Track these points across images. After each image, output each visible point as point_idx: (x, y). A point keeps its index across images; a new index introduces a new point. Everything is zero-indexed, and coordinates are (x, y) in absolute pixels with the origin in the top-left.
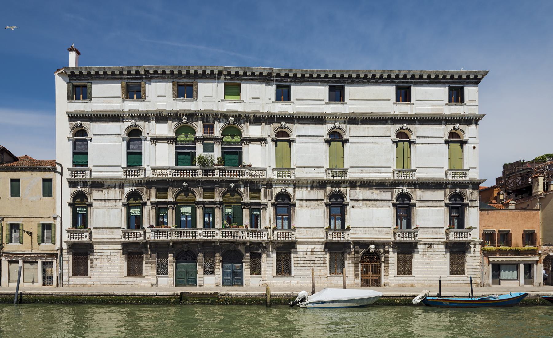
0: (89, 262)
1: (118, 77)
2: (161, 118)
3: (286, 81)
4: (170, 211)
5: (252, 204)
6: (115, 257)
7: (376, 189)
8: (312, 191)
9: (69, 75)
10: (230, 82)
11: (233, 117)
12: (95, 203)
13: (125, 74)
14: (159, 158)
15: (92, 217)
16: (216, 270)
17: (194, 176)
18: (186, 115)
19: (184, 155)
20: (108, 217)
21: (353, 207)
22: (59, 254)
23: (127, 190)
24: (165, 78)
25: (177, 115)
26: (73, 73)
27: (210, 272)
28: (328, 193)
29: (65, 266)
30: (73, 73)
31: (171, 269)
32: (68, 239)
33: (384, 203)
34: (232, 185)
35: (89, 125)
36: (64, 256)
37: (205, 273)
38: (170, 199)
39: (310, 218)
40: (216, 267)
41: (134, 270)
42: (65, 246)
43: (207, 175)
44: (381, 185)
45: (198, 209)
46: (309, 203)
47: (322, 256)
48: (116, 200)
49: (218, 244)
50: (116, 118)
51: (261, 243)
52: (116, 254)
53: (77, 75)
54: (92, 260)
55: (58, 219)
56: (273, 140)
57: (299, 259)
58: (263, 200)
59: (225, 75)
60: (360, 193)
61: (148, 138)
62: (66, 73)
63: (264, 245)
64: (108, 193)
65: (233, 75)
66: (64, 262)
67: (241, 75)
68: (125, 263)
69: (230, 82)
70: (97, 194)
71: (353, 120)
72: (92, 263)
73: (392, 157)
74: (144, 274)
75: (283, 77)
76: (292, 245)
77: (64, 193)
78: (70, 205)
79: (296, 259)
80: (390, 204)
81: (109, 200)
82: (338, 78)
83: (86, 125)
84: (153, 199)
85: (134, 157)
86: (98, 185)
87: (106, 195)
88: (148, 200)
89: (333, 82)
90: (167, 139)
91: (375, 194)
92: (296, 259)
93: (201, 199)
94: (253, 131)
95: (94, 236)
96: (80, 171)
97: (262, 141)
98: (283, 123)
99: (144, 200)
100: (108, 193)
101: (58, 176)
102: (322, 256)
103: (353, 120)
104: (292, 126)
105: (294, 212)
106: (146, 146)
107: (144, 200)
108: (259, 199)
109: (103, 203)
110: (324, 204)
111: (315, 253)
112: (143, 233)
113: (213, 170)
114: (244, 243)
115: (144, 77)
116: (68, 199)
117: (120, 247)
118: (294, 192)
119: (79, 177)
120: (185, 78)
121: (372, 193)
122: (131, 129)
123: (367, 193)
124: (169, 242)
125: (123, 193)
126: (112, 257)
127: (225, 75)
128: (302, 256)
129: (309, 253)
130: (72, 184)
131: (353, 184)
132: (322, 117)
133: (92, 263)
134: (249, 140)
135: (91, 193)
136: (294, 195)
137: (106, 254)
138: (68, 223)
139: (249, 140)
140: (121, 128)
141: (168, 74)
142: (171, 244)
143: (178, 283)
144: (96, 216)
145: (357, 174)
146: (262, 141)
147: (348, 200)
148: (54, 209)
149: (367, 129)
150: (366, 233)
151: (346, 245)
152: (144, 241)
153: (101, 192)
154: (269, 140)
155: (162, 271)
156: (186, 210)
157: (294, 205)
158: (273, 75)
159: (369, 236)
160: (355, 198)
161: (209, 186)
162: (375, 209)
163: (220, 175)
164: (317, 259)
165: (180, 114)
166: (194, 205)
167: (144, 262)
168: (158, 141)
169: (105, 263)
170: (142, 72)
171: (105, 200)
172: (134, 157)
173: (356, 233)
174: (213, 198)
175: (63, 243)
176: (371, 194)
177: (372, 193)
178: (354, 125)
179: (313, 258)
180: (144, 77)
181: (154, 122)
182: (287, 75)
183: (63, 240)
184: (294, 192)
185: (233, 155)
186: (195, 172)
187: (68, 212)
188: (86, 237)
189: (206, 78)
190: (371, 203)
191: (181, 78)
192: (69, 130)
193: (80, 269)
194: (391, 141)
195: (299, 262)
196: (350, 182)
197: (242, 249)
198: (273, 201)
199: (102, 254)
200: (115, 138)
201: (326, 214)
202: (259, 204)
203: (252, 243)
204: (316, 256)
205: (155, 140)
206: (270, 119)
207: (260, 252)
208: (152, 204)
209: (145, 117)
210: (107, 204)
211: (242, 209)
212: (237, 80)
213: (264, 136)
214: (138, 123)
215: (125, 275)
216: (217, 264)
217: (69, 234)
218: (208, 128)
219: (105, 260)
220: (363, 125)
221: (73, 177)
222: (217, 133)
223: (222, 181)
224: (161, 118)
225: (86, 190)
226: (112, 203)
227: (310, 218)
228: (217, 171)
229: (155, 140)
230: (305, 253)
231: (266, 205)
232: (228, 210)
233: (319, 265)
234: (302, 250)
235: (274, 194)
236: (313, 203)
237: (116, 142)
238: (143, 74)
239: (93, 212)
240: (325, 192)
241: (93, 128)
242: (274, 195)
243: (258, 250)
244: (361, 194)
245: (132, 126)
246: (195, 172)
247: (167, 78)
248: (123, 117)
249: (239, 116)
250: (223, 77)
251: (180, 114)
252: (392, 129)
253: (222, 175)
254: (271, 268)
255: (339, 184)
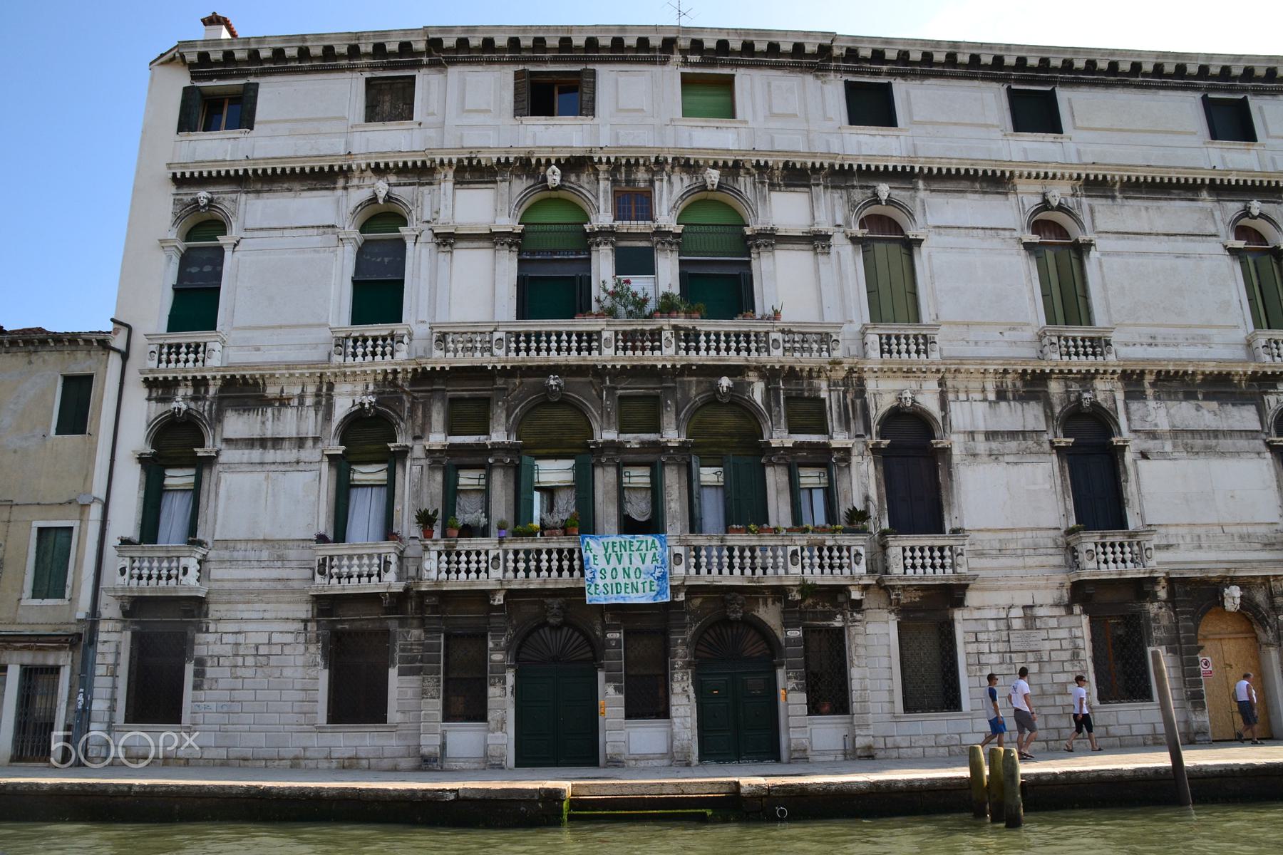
0: (189, 669)
1: (344, 62)
2: (472, 172)
3: (877, 74)
4: (498, 478)
5: (798, 447)
6: (287, 650)
7: (1207, 397)
8: (1003, 404)
9: (191, 65)
10: (698, 71)
11: (715, 166)
12: (228, 455)
13: (367, 55)
14: (464, 295)
15: (212, 504)
16: (674, 700)
17: (584, 353)
18: (558, 163)
19: (550, 286)
20: (268, 500)
21: (1144, 455)
22: (85, 638)
23: (342, 407)
24: (490, 62)
25: (529, 160)
26: (204, 56)
27: (647, 702)
28: (1058, 410)
29: (101, 684)
30: (204, 56)
31: (502, 699)
32: (122, 581)
33: (1242, 443)
34: (725, 382)
35: (234, 201)
36: (100, 648)
37: (633, 712)
38: (498, 436)
39: (1006, 498)
40: (677, 687)
41: (356, 699)
42: (110, 609)
43: (634, 349)
44: (1219, 386)
45: (598, 472)
46: (994, 445)
47: (1063, 633)
48: (300, 442)
49: (681, 597)
50: (323, 177)
51: (844, 589)
52: (289, 638)
53: (217, 63)
54: (200, 663)
55: (95, 512)
56: (854, 240)
57: (985, 648)
58: (839, 439)
59: (684, 52)
60: (1160, 414)
61: (427, 236)
62: (182, 56)
63: (856, 595)
64: (276, 418)
65: (710, 50)
66: (100, 670)
67: (734, 52)
68: (324, 676)
69: (698, 71)
70: (236, 424)
71: (1097, 186)
72: (200, 674)
73: (1235, 299)
74: (393, 715)
75: (865, 60)
76: (954, 594)
77: (128, 420)
78: (142, 459)
79: (973, 648)
80: (1259, 444)
81: (277, 442)
82: (1032, 69)
83: (227, 198)
84: (437, 439)
85: (378, 295)
86: (244, 392)
87: (269, 424)
88: (416, 438)
89: (1019, 81)
90: (494, 238)
91: (1205, 415)
92: (973, 648)
93: (611, 435)
94: (786, 210)
95: (216, 573)
96: (188, 346)
97: (816, 241)
98: (884, 189)
99: (402, 441)
100: (276, 418)
101: (114, 361)
102: (1063, 633)
103: (1097, 186)
104: (913, 198)
105: (950, 475)
106: (419, 261)
107: (402, 441)
108: (823, 430)
109: (256, 454)
110: (1047, 446)
111: (1038, 623)
112: (393, 558)
113: (652, 333)
114: (779, 592)
115: (425, 59)
116: (135, 438)
117: (304, 611)
118: (944, 405)
119: (186, 368)
120: (555, 60)
121: (1198, 408)
122: (371, 210)
123: (1186, 413)
124: (494, 592)
125: (328, 416)
126: (277, 650)
127: (684, 52)
128: (993, 636)
129: (1017, 624)
130: (160, 388)
131: (1132, 381)
132: (1003, 173)
133: (200, 674)
134: (772, 239)
135: (218, 419)
136: (944, 418)
137: (253, 639)
138: (126, 520)
139: (772, 239)
140: (335, 208)
141: (501, 49)
142: (499, 599)
143: (528, 757)
144: (228, 498)
145: (1138, 348)
146: (816, 241)
147: (1124, 434)
148: (87, 477)
149: (1143, 212)
150: (1200, 547)
151: (1141, 588)
152: (398, 587)
153: (252, 416)
154: (838, 241)
155: (466, 703)
156: (554, 472)
157: (946, 451)
158: (836, 52)
159: (1212, 556)
160: (1147, 427)
161: (643, 395)
162: (1216, 466)
163: (678, 348)
164: (1047, 645)
165: (539, 160)
166: (588, 457)
167: (393, 673)
168: (459, 245)
169: (248, 673)
170: (420, 46)
171: (262, 443)
172: (378, 295)
173: (1168, 547)
174: (657, 429)
175: (104, 598)
176: (1194, 412)
177: (1198, 408)
178: (1103, 201)
179: (1037, 639)
180: (425, 59)
181: (450, 185)
182: (878, 56)
183: (105, 583)
184: (944, 405)
185: (721, 285)
186: (590, 341)
187: (130, 482)
188: (185, 571)
189: (624, 61)
190: (1198, 442)
191: (544, 62)
192: (170, 218)
193: (155, 698)
194: (1222, 251)
195: (984, 659)
196: (1124, 372)
197: (769, 614)
198: (873, 439)
199: (241, 638)
200: (316, 239)
201: (1059, 482)
202: (825, 449)
203: (808, 590)
204: (1043, 634)
205: (447, 240)
206: (841, 176)
207: (838, 623)
208: (430, 453)
209: (421, 172)
210: (271, 455)
211: (763, 466)
212: (723, 65)
213: (824, 226)
214: (397, 191)
215: (322, 717)
216: (678, 676)
217: (127, 563)
218: (634, 202)
219: (250, 661)
220: (1131, 202)
221: (163, 365)
222: (666, 217)
223: (687, 369)
224: (472, 172)
225: (204, 407)
226: (289, 454)
227: (1006, 498)
228: (667, 334)
229: (447, 240)
230: (1002, 625)
231: (847, 451)
232: (709, 475)
233: (1056, 667)
234: (992, 613)
235: (873, 412)
236: (1013, 445)
237: (316, 250)
238: (421, 53)
239: (217, 485)
240: (1048, 405)
241: (250, 212)
242: (876, 414)
243: (831, 617)
244: (1162, 412)
245: (374, 200)
246: (590, 341)
247: (500, 62)
248: (346, 173)
249: (736, 162)
250: (677, 57)
251: (539, 160)
252: (1217, 214)
253: (687, 349)
254: (886, 684)
255: (1087, 378)
